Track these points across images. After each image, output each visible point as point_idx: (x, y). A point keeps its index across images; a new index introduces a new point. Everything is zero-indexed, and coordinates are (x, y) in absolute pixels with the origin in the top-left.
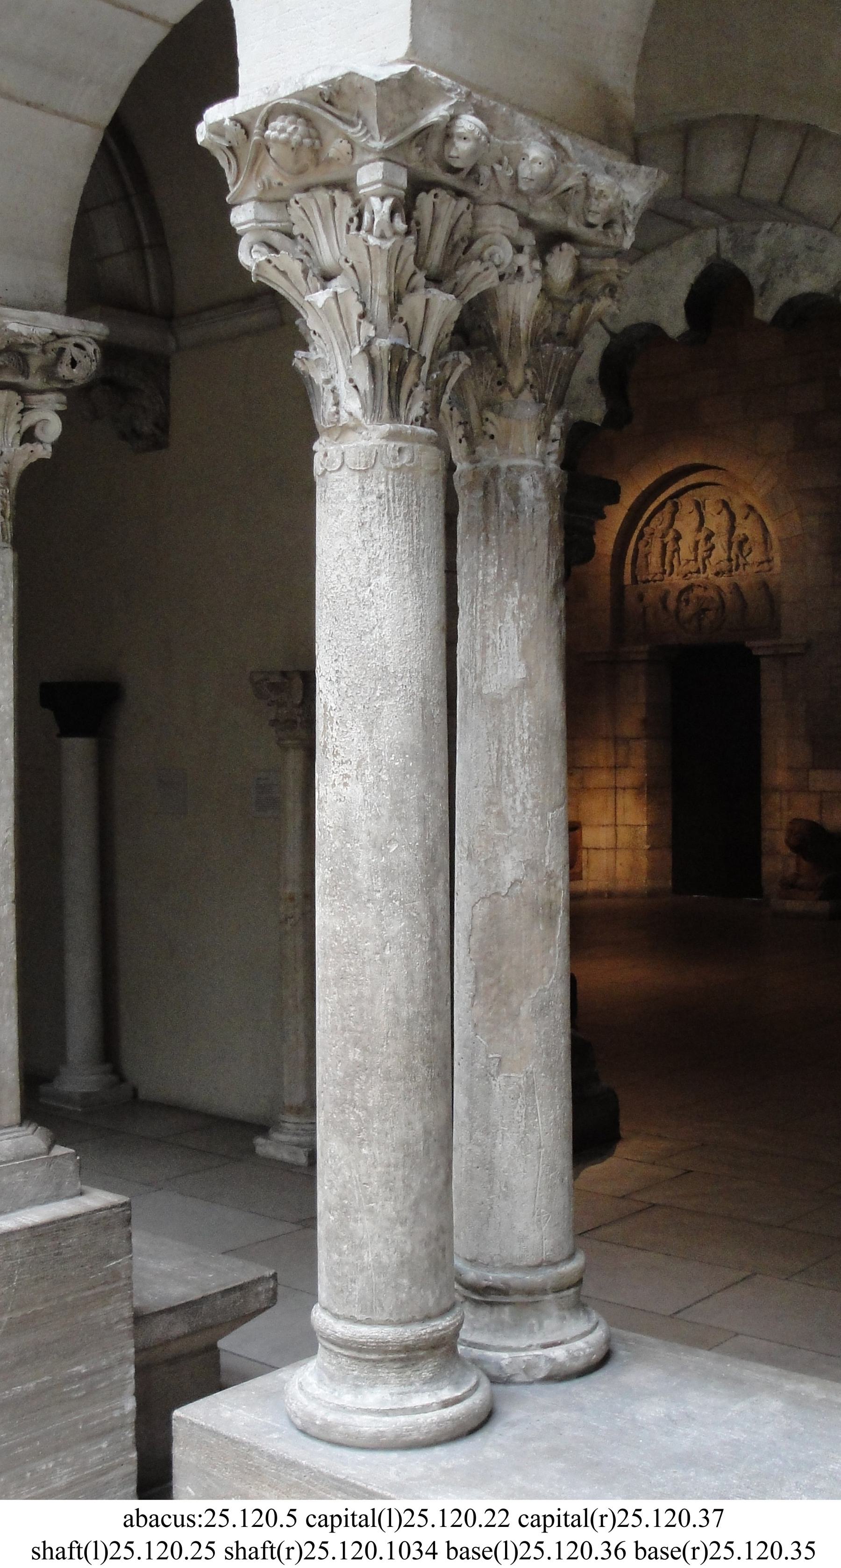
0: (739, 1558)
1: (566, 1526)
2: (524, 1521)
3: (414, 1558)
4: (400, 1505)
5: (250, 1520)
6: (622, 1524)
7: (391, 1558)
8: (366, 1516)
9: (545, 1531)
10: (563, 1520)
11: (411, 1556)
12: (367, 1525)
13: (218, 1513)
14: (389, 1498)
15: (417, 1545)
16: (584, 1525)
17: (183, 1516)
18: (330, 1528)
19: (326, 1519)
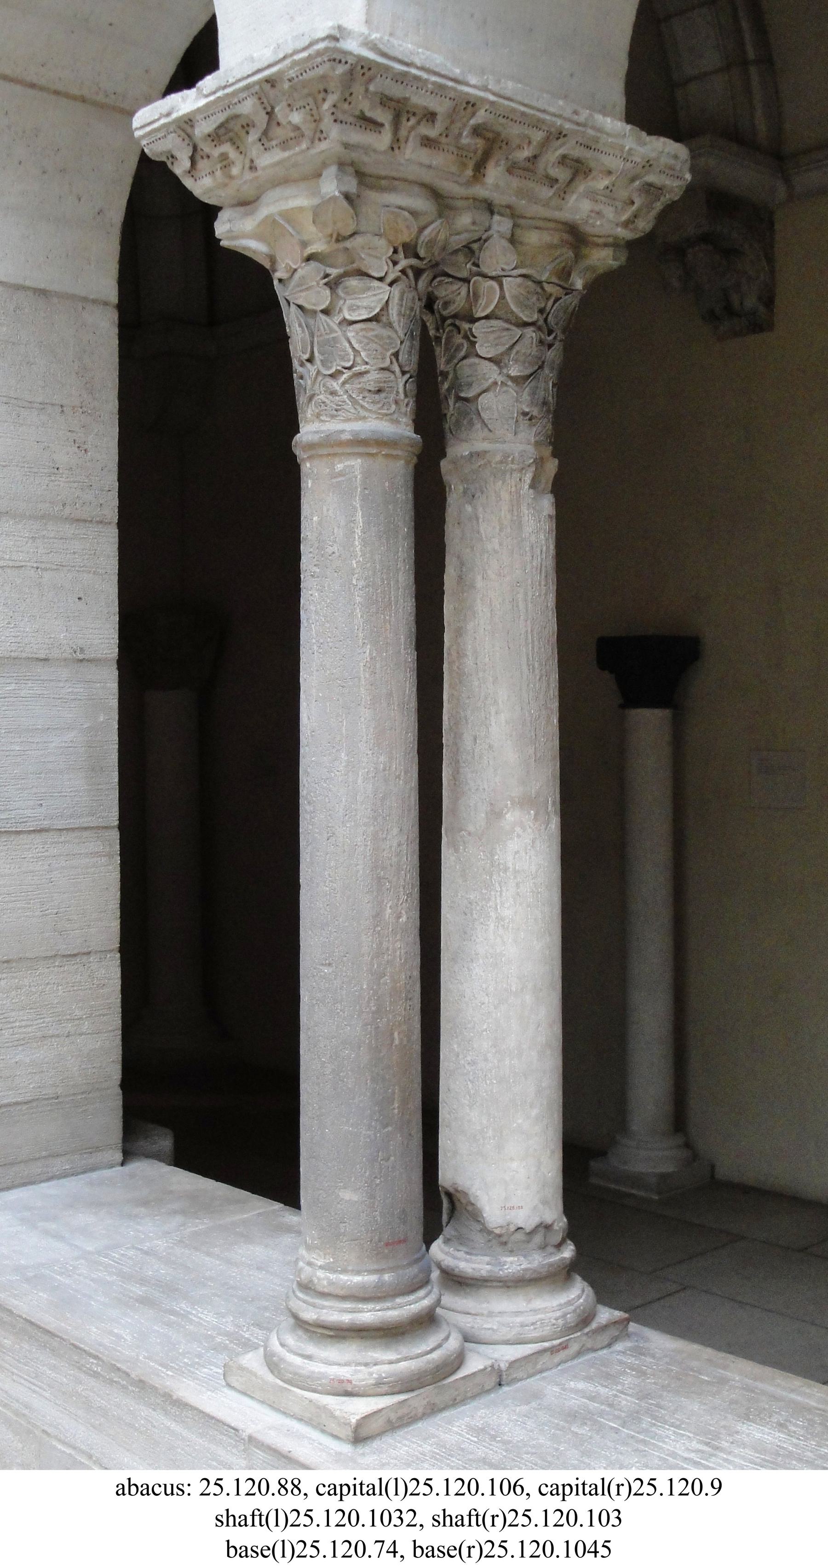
0: (581, 1525)
1: (362, 1494)
2: (322, 1490)
3: (395, 1526)
4: (407, 1475)
5: (453, 1489)
6: (638, 1493)
7: (373, 1525)
8: (596, 1486)
9: (341, 1500)
10: (581, 1489)
11: (393, 1523)
12: (596, 1494)
13: (422, 1482)
14: (683, 1468)
15: (616, 1513)
16: (601, 1493)
17: (172, 1485)
18: (338, 1496)
19: (335, 1488)
